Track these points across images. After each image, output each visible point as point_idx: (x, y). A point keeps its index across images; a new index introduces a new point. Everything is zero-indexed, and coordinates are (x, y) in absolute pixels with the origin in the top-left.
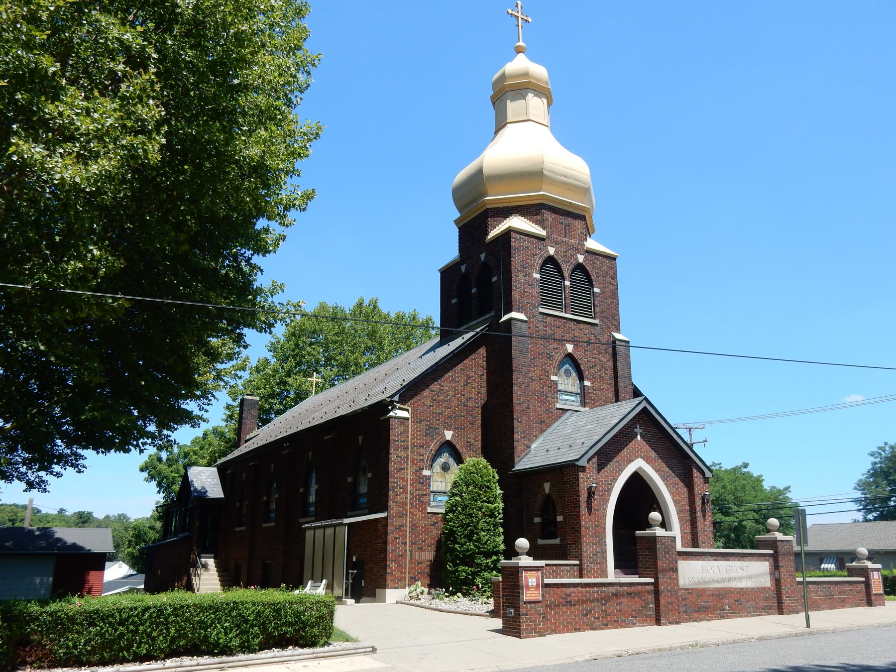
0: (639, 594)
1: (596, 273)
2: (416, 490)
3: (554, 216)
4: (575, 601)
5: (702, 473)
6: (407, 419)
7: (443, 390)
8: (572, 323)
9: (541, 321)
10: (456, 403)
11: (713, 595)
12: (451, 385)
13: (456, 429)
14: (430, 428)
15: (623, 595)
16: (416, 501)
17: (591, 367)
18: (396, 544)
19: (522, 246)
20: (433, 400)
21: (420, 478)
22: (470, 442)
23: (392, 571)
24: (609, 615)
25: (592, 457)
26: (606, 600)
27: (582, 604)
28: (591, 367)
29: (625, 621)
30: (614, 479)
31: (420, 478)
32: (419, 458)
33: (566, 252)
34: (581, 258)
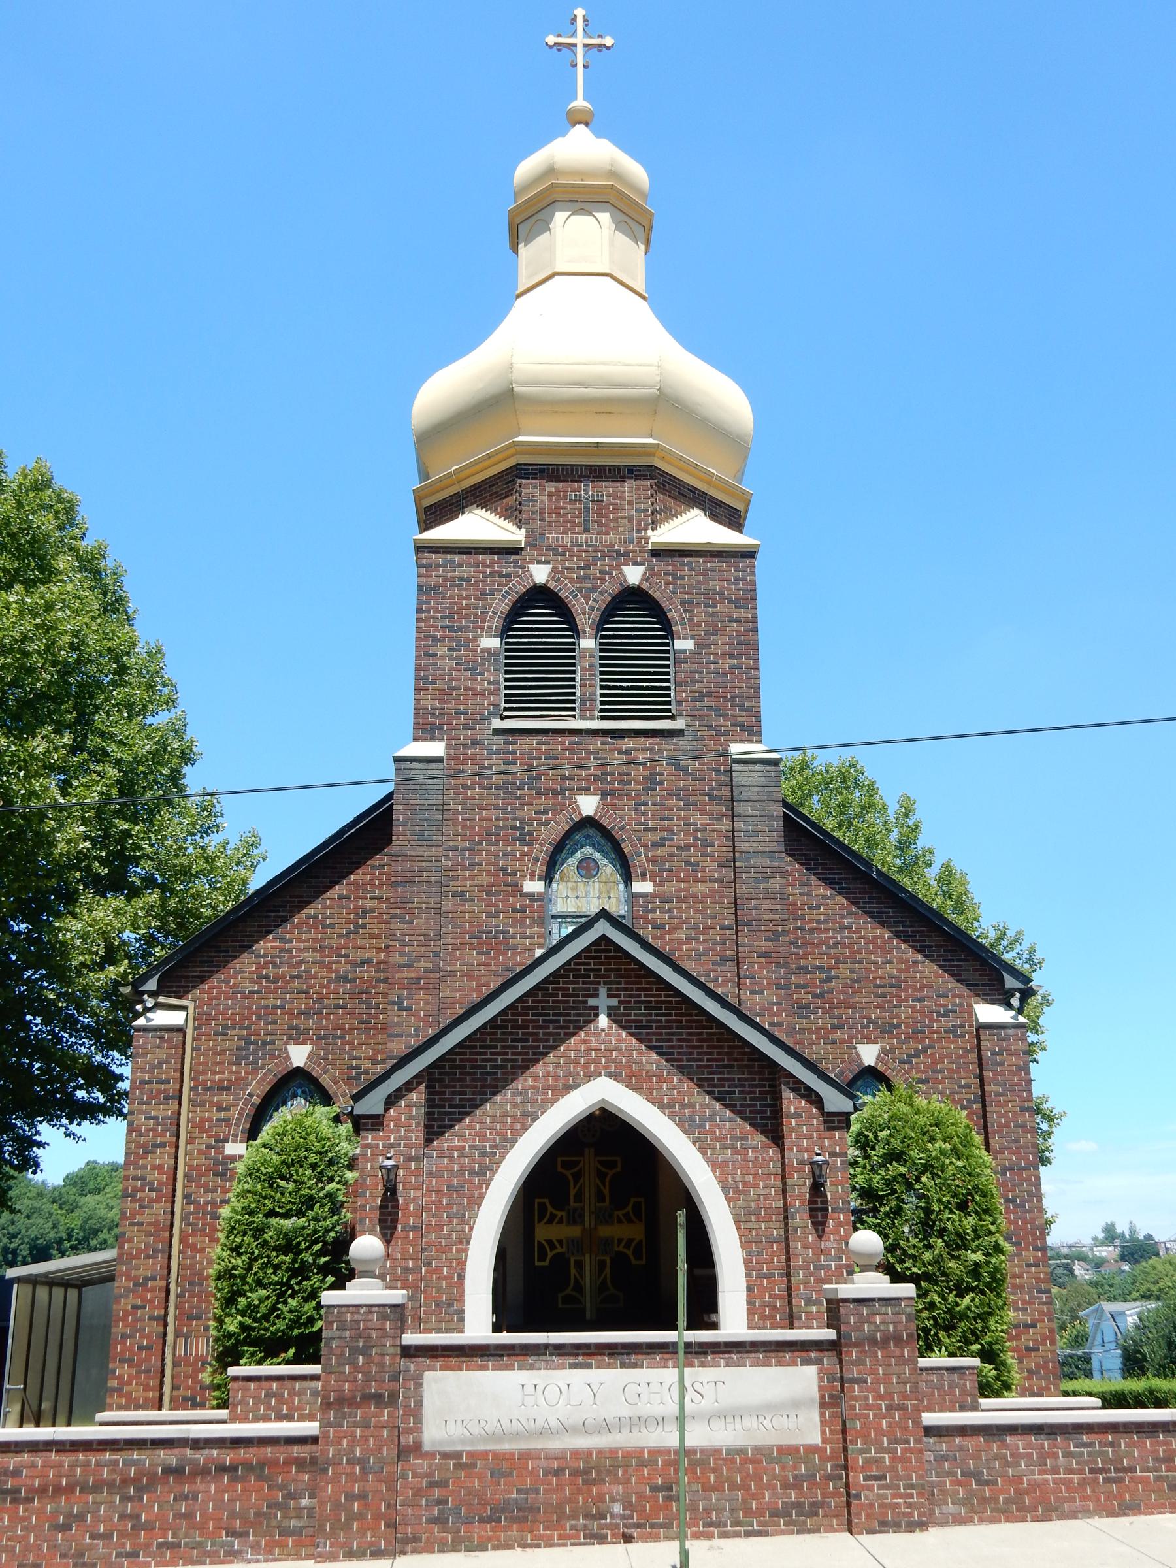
0: (258, 1469)
1: (684, 602)
2: (207, 1191)
3: (550, 487)
4: (30, 1489)
5: (816, 1100)
6: (180, 1030)
7: (289, 951)
8: (598, 741)
9: (498, 752)
10: (324, 976)
11: (558, 1472)
12: (313, 936)
13: (319, 1038)
14: (248, 1043)
15: (204, 1472)
16: (204, 1219)
17: (655, 845)
18: (136, 1320)
19: (452, 581)
20: (260, 976)
21: (217, 1163)
22: (358, 1067)
23: (122, 1383)
24: (149, 1527)
25: (408, 1087)
26: (145, 1483)
27: (53, 1496)
28: (655, 845)
29: (200, 1544)
30: (505, 1140)
31: (217, 1163)
32: (215, 1115)
33: (587, 567)
34: (633, 575)
